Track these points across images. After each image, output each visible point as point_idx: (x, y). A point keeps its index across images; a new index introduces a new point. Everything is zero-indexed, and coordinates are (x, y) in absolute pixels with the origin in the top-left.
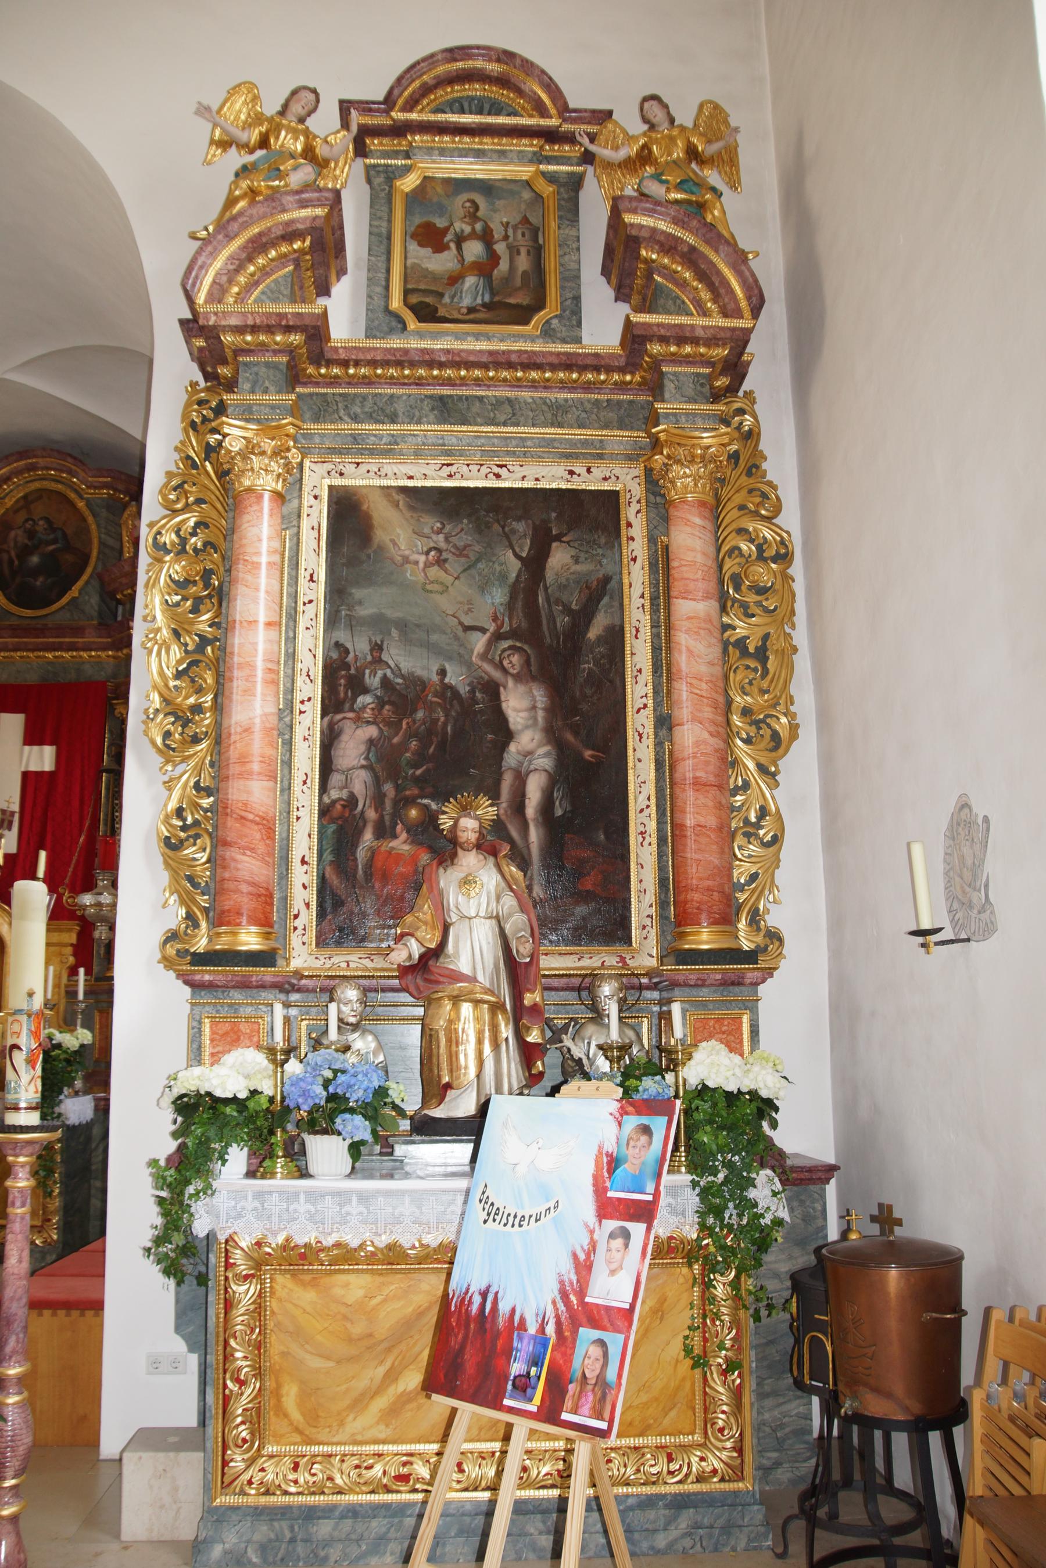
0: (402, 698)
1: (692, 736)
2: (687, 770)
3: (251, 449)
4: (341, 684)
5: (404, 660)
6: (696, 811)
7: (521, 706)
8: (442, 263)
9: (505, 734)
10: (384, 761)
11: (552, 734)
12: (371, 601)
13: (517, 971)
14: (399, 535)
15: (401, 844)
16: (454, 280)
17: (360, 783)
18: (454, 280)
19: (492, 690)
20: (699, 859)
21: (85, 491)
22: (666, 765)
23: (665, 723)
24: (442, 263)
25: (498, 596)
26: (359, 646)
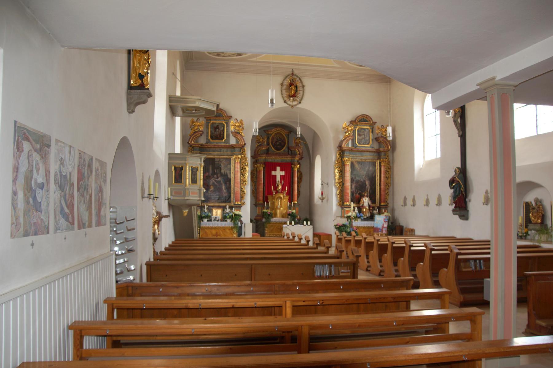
0: (357, 182)
1: (382, 187)
2: (382, 190)
3: (347, 160)
4: (352, 180)
5: (357, 178)
6: (383, 193)
7: (367, 183)
8: (360, 138)
9: (366, 185)
10: (356, 188)
11: (370, 185)
12: (355, 173)
13: (369, 206)
14: (357, 166)
15: (357, 195)
16: (361, 140)
17: (354, 189)
18: (361, 140)
19: (365, 181)
20: (383, 198)
21: (284, 133)
22: (380, 189)
23: (380, 185)
24: (360, 138)
25: (365, 173)
26: (354, 177)
